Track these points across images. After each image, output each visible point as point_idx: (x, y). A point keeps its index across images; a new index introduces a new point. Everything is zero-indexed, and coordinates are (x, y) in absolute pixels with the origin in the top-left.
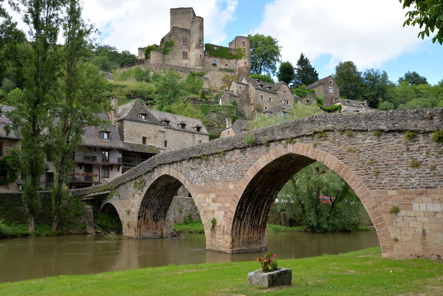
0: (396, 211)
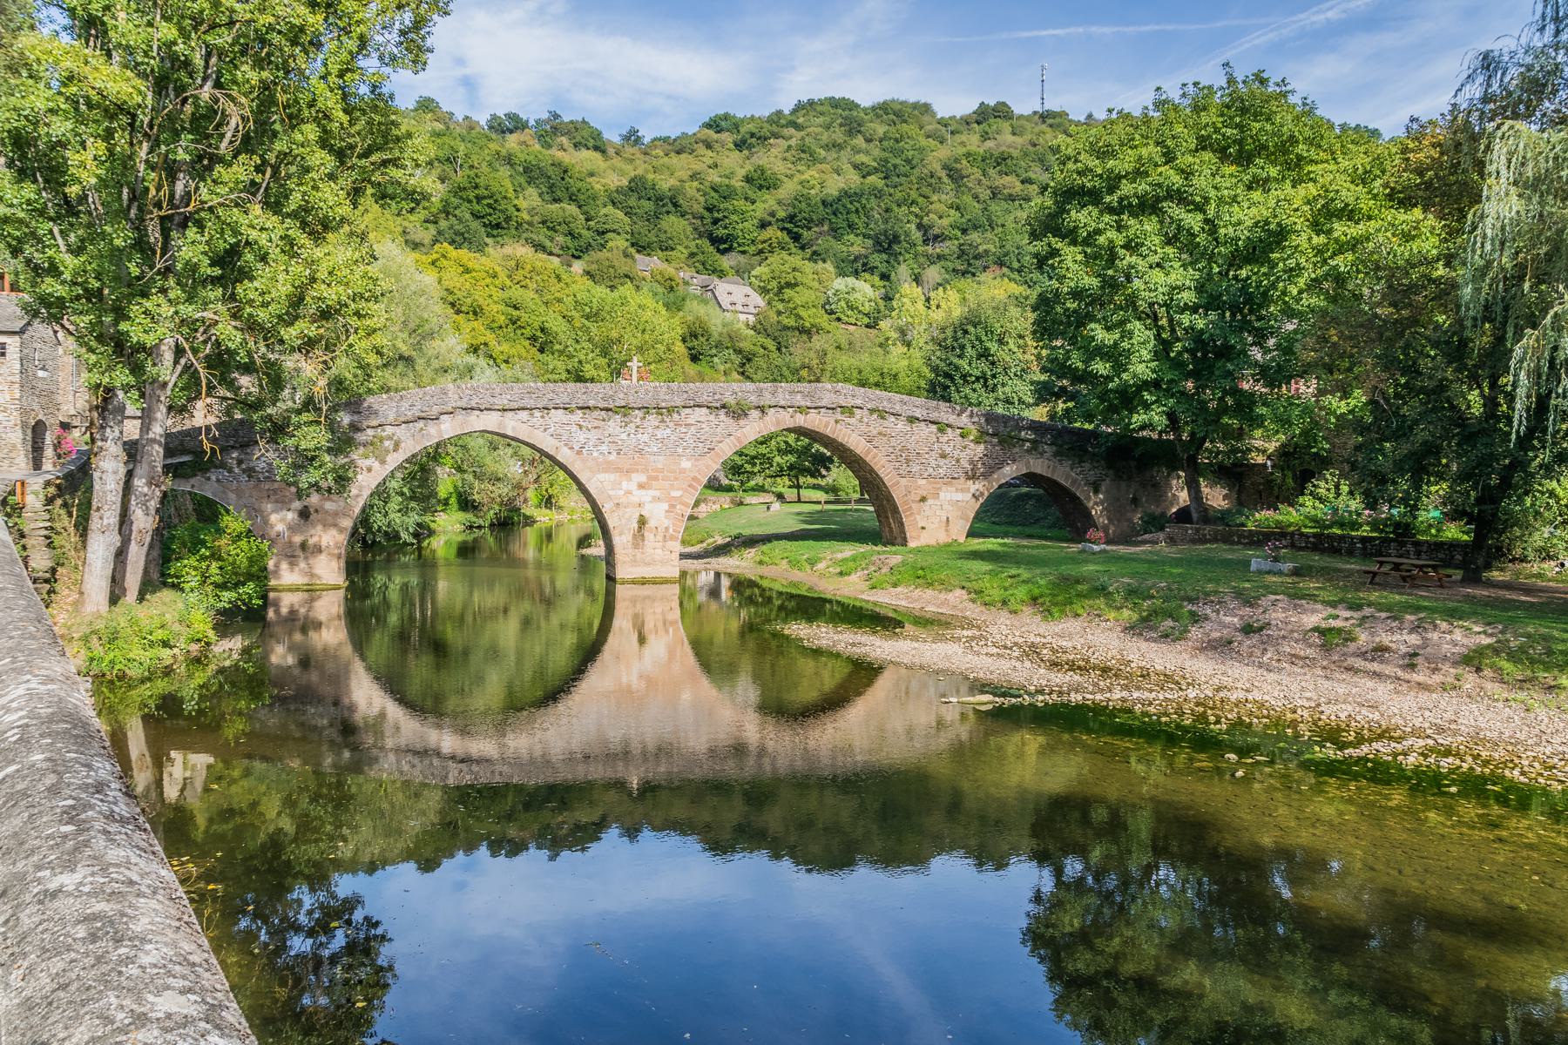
0: (923, 499)
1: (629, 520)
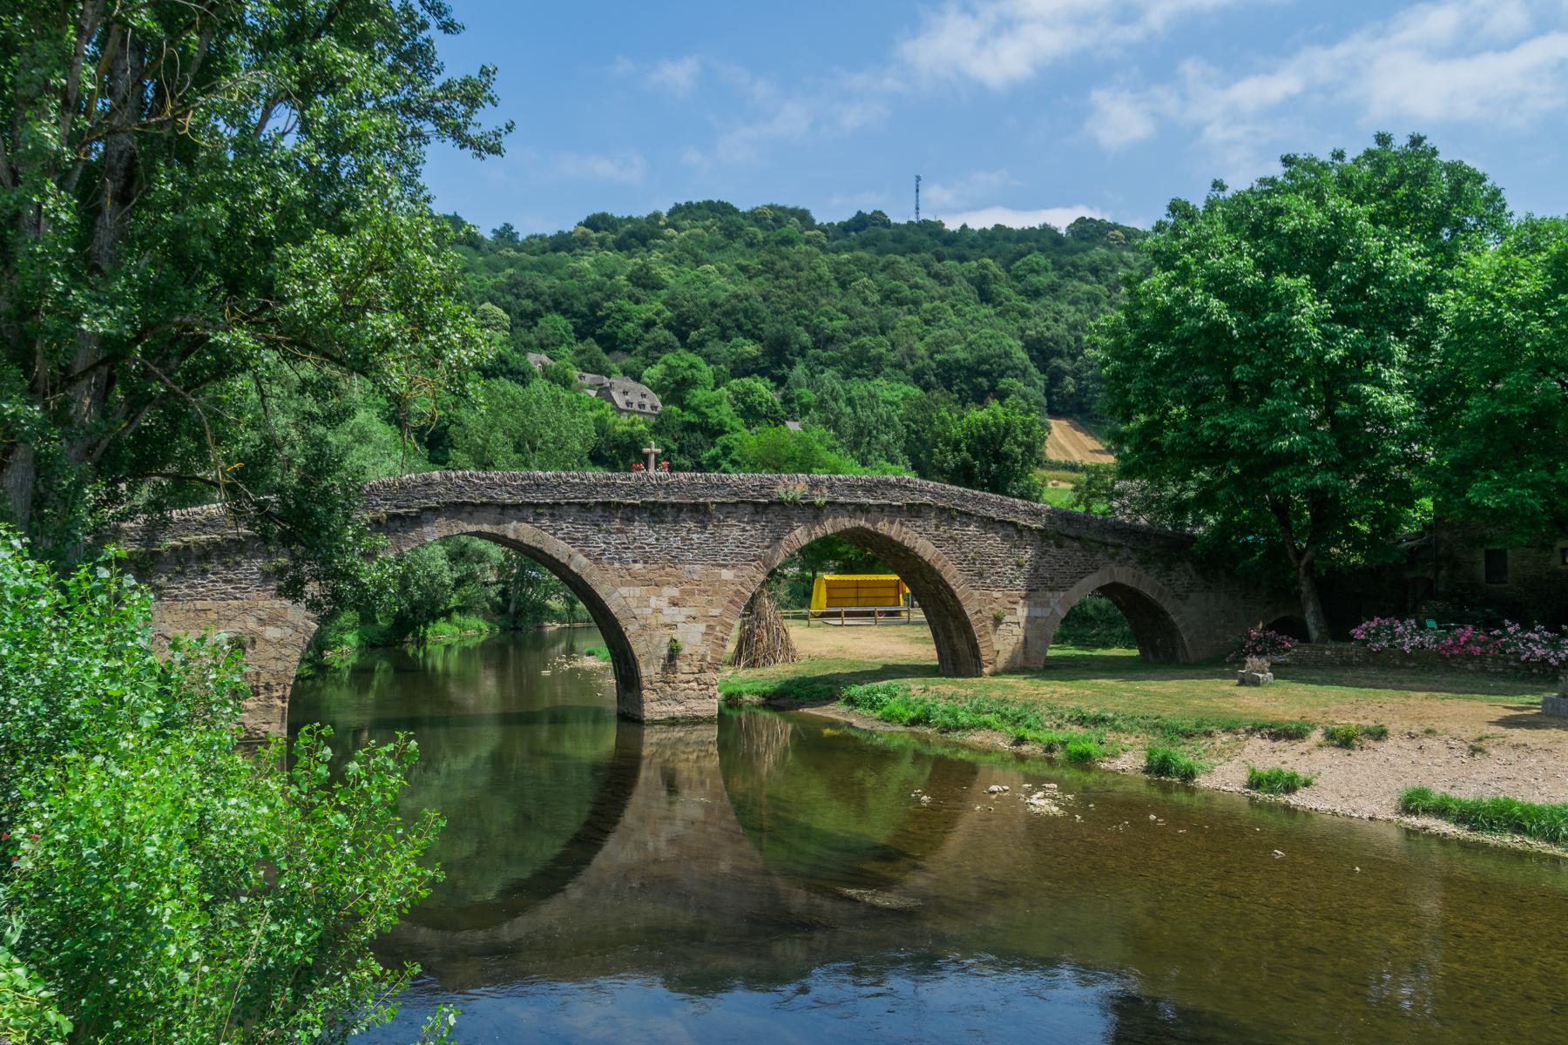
1: (658, 646)
